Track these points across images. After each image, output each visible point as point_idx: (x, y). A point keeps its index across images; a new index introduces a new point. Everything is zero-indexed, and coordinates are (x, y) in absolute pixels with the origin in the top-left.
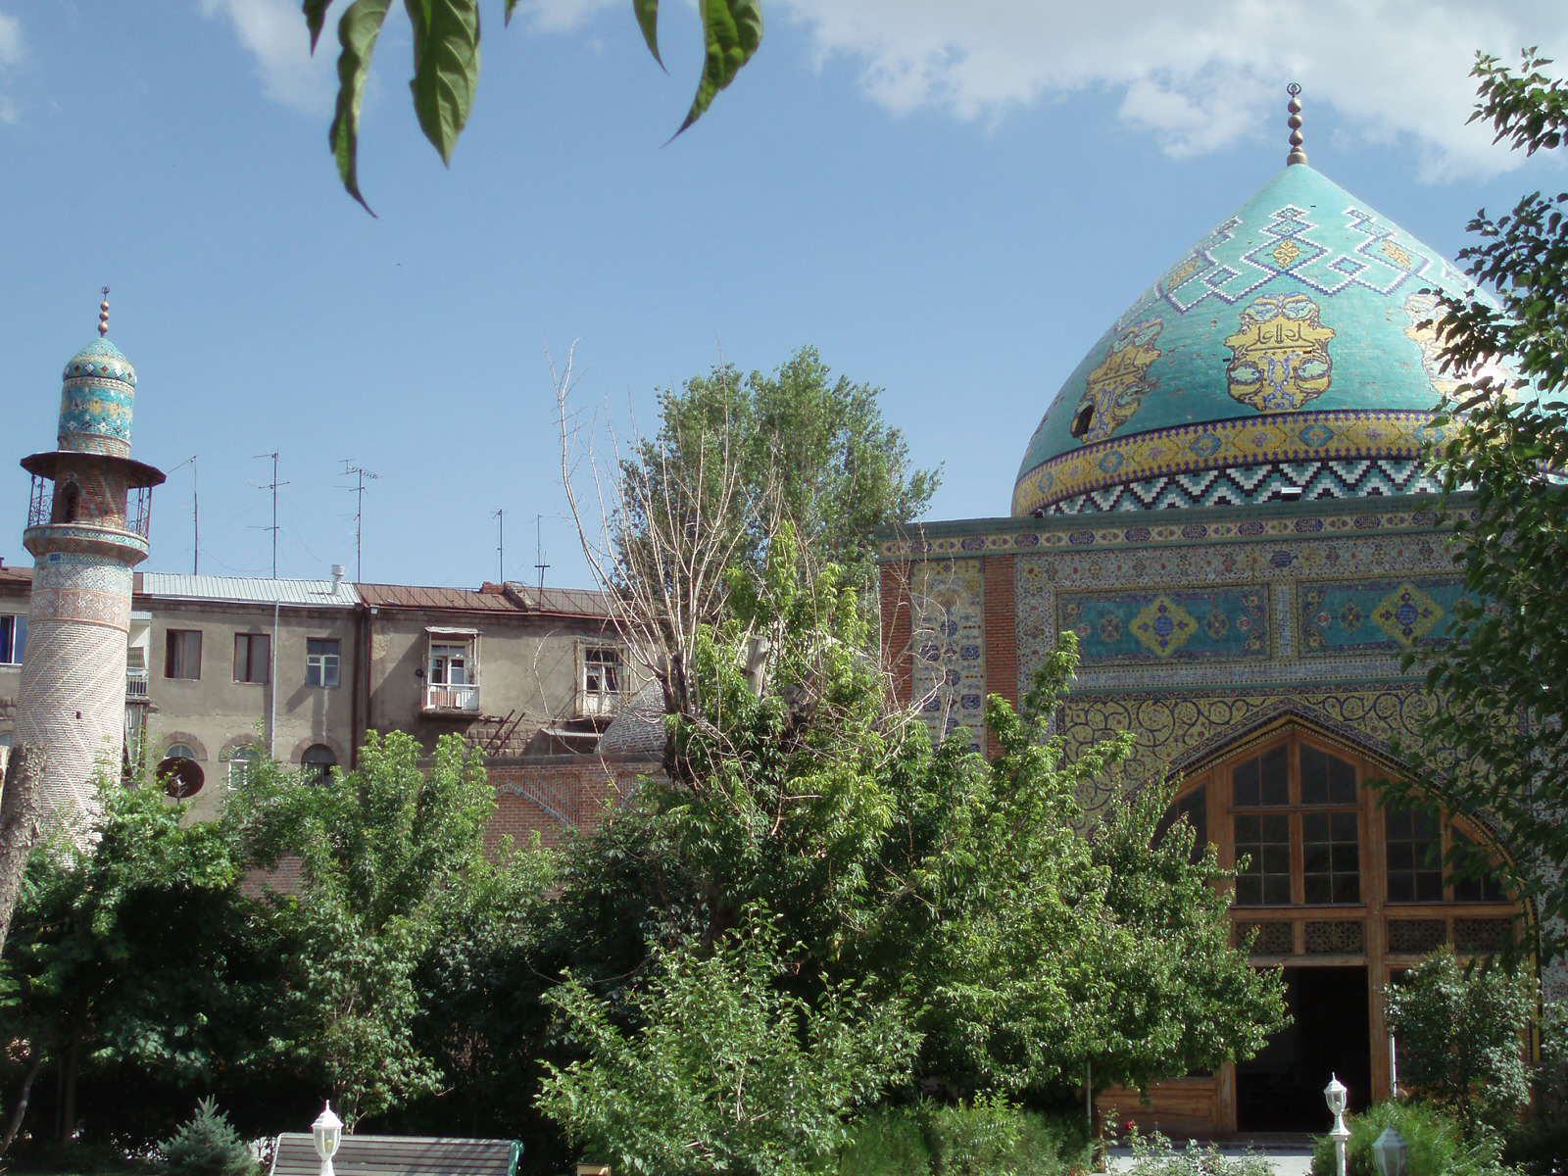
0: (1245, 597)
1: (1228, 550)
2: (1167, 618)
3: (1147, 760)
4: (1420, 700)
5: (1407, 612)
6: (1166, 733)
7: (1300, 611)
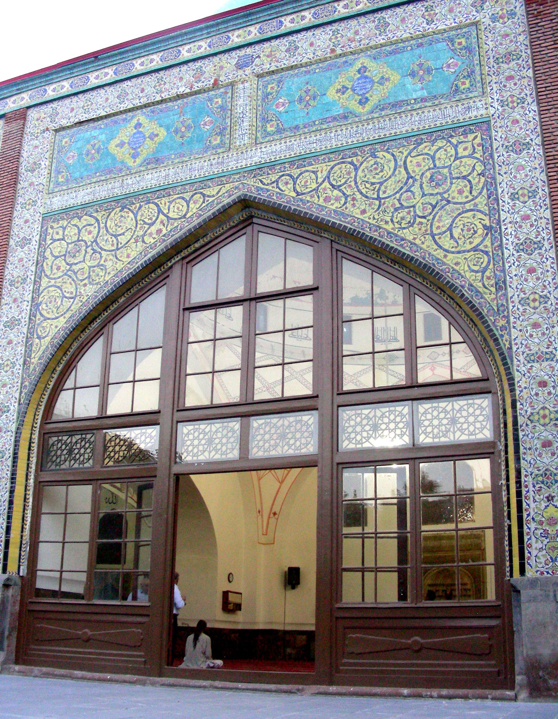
0: (210, 100)
2: (141, 132)
3: (109, 264)
6: (128, 235)
7: (259, 102)
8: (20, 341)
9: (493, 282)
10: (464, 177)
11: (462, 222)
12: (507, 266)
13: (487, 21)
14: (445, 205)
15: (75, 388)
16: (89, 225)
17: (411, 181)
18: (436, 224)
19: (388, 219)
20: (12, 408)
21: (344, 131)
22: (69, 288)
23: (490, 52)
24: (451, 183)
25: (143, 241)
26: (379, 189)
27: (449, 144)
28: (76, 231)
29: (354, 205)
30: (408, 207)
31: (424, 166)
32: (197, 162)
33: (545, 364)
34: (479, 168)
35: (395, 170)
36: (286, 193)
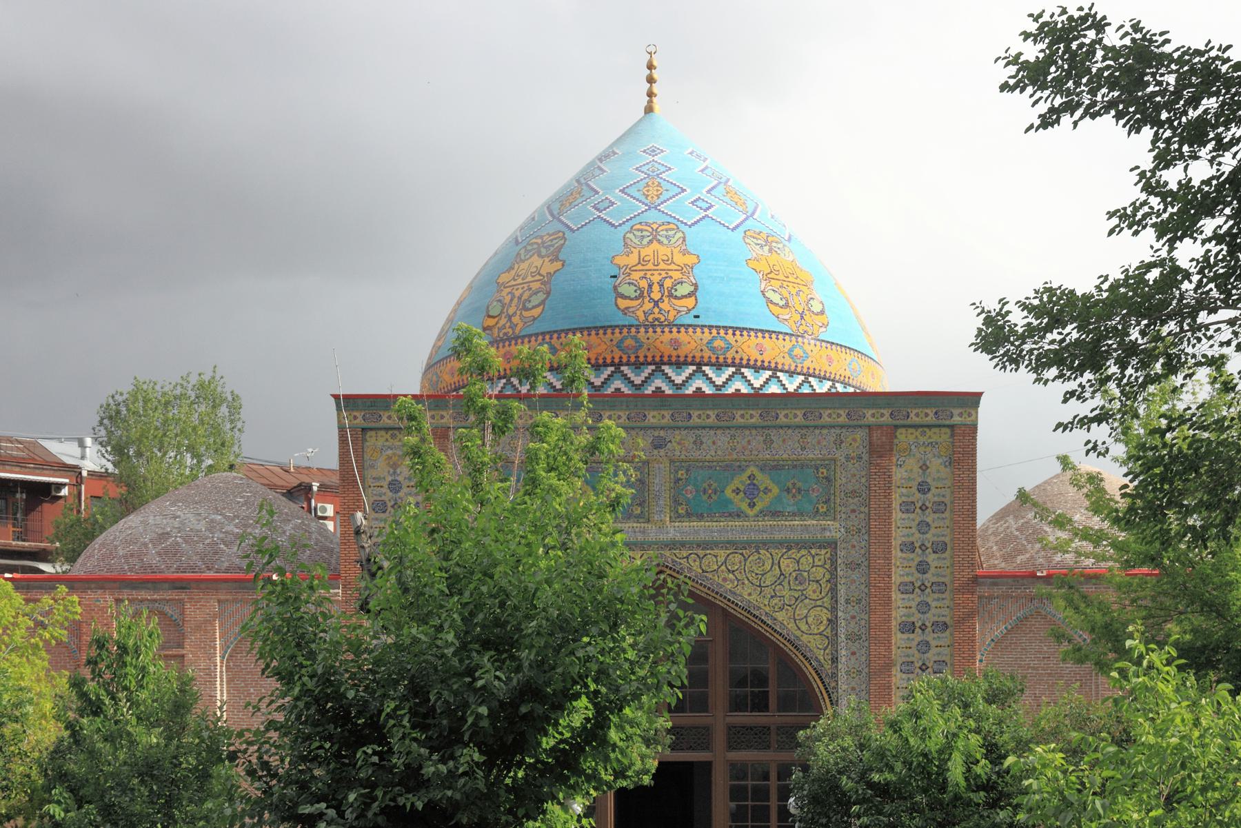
4: (759, 558)
5: (752, 491)
9: (830, 657)
10: (817, 581)
18: (797, 612)
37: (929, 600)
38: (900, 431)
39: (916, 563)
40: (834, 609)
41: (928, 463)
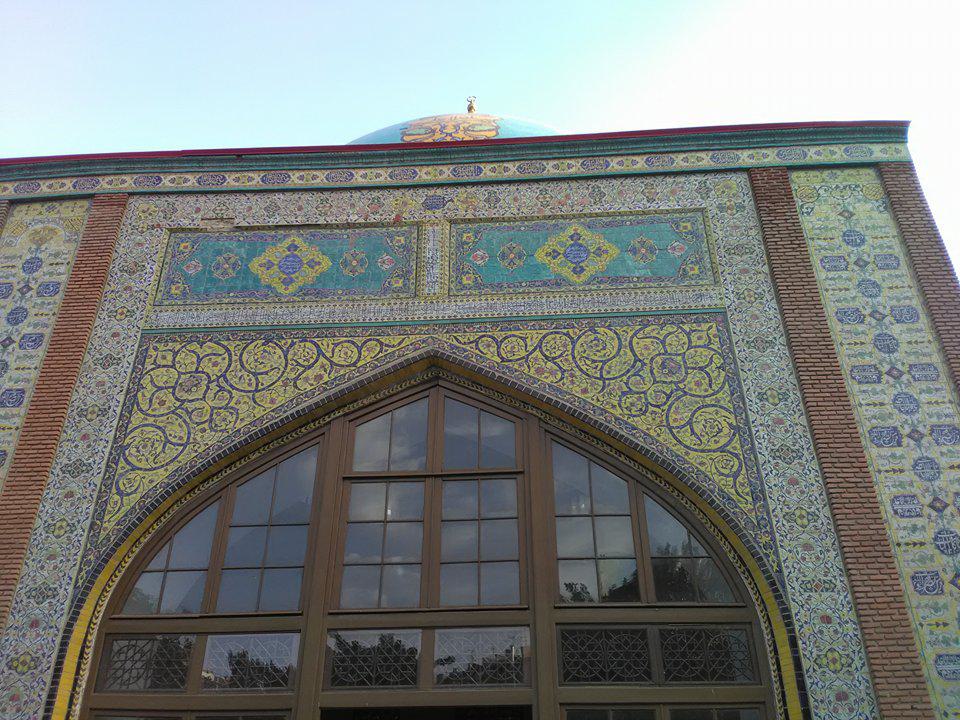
0: (391, 237)
1: (375, 194)
2: (295, 256)
3: (243, 408)
5: (577, 252)
6: (274, 375)
8: (87, 495)
9: (748, 490)
10: (701, 369)
11: (702, 417)
12: (763, 474)
13: (716, 211)
14: (682, 396)
15: (166, 571)
16: (214, 354)
17: (639, 364)
18: (673, 416)
19: (616, 403)
20: (61, 592)
21: (557, 299)
22: (177, 430)
23: (720, 241)
24: (687, 373)
25: (296, 387)
26: (602, 368)
27: (680, 330)
28: (195, 359)
29: (572, 382)
30: (638, 393)
31: (654, 350)
32: (374, 303)
33: (825, 595)
34: (718, 361)
35: (619, 350)
36: (488, 356)
37: (910, 391)
38: (794, 175)
39: (871, 337)
40: (740, 407)
41: (851, 208)
